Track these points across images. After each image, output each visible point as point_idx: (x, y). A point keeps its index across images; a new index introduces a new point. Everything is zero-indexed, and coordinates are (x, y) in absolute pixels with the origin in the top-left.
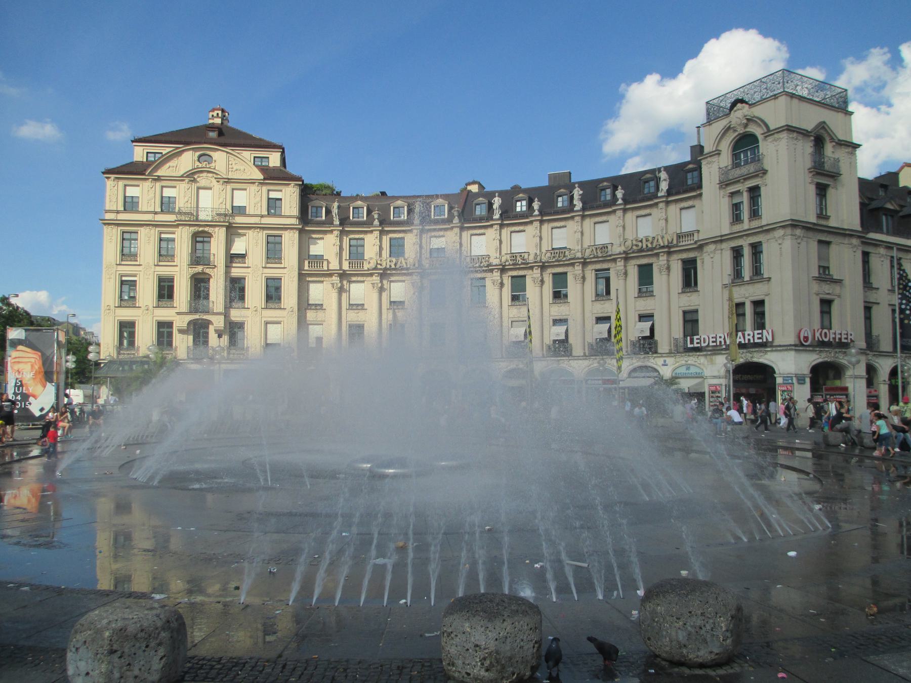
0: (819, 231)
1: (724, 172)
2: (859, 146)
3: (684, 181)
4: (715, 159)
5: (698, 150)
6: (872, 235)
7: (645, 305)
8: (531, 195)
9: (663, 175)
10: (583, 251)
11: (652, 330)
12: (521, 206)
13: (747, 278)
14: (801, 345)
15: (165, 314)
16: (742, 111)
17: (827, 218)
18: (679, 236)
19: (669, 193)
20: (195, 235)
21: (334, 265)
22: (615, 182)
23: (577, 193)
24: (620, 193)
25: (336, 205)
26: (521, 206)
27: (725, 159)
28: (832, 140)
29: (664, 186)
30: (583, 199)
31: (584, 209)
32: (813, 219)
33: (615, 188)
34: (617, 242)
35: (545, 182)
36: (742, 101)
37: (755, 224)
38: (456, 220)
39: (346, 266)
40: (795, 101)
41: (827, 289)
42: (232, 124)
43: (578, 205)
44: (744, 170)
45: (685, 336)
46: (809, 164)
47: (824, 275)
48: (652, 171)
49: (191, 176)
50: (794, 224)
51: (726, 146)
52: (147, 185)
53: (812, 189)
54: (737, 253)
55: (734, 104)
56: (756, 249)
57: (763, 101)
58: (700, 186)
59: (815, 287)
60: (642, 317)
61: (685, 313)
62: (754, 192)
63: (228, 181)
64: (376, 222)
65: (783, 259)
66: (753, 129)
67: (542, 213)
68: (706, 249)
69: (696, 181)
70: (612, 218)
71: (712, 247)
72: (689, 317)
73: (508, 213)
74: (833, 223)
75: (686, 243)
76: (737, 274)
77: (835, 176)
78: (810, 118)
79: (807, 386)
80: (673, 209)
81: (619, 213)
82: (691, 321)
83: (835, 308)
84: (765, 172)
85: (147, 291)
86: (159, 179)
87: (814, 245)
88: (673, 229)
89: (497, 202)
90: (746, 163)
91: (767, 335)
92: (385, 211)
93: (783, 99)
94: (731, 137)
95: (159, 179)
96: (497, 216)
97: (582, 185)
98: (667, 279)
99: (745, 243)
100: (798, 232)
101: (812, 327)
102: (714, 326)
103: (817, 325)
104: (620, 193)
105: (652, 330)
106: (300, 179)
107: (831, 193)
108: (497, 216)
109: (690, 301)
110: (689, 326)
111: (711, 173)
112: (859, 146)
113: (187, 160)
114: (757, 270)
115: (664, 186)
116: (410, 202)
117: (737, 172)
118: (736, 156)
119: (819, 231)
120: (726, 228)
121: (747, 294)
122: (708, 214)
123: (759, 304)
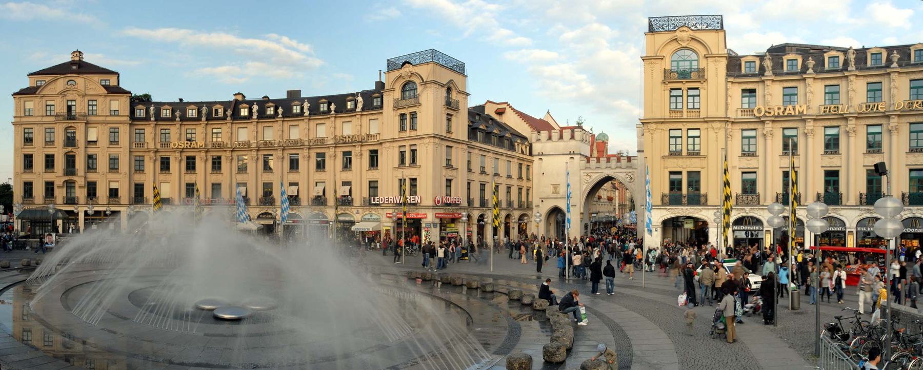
0: (446, 140)
1: (396, 101)
2: (469, 94)
3: (371, 101)
4: (391, 93)
5: (380, 85)
6: (474, 143)
7: (347, 176)
8: (277, 103)
9: (360, 99)
10: (309, 141)
11: (350, 191)
12: (271, 111)
13: (407, 165)
14: (434, 207)
16: (408, 69)
17: (451, 133)
18: (368, 136)
19: (363, 109)
21: (151, 146)
22: (330, 100)
23: (306, 105)
24: (333, 107)
25: (152, 108)
26: (271, 111)
27: (397, 94)
28: (456, 90)
29: (360, 106)
30: (309, 109)
31: (310, 115)
32: (444, 134)
33: (330, 104)
35: (284, 96)
36: (409, 63)
37: (413, 133)
38: (229, 118)
39: (159, 146)
40: (438, 67)
41: (449, 173)
42: (87, 58)
43: (307, 113)
44: (409, 102)
45: (370, 196)
46: (444, 103)
47: (449, 166)
48: (353, 95)
49: (63, 94)
50: (435, 136)
51: (398, 87)
52: (37, 100)
53: (445, 117)
55: (404, 64)
57: (420, 64)
58: (381, 107)
59: (444, 171)
60: (345, 183)
61: (370, 182)
63: (85, 95)
64: (178, 119)
65: (427, 153)
66: (414, 79)
67: (284, 116)
68: (384, 145)
69: (379, 104)
70: (328, 122)
71: (388, 144)
72: (372, 185)
73: (262, 115)
74: (454, 136)
75: (372, 141)
76: (402, 161)
77: (456, 109)
78: (446, 76)
79: (438, 229)
80: (365, 119)
81: (332, 119)
82: (373, 187)
83: (453, 183)
84: (420, 105)
86: (44, 96)
87: (444, 148)
88: (365, 132)
89: (255, 108)
90: (410, 98)
91: (418, 199)
92: (184, 112)
93: (431, 65)
94: (401, 82)
95: (44, 96)
96: (255, 116)
97: (310, 100)
98: (360, 161)
100: (437, 140)
101: (441, 195)
102: (388, 192)
103: (444, 194)
104: (333, 107)
105: (350, 191)
106: (129, 93)
107: (453, 119)
108: (255, 116)
109: (373, 175)
110: (372, 190)
111: (388, 100)
112: (469, 94)
113: (61, 83)
114: (413, 160)
115: (360, 106)
116: (199, 105)
117: (404, 103)
119: (446, 140)
120: (396, 134)
122: (384, 125)
123: (413, 180)
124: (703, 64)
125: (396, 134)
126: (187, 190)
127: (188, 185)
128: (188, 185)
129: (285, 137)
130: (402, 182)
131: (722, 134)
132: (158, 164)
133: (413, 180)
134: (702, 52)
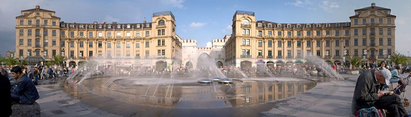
15: (30, 48)
20: (36, 30)
27: (157, 24)
34: (132, 36)
51: (157, 21)
54: (159, 41)
56: (163, 41)
62: (163, 30)
66: (163, 19)
76: (159, 45)
82: (147, 52)
85: (25, 42)
94: (159, 20)
99: (161, 39)
118: (159, 23)
120: (157, 36)
121: (161, 48)
124: (250, 24)
125: (157, 36)
126: (90, 54)
127: (90, 52)
128: (90, 52)
129: (125, 35)
130: (159, 51)
131: (255, 41)
132: (98, 44)
133: (163, 50)
134: (250, 21)
